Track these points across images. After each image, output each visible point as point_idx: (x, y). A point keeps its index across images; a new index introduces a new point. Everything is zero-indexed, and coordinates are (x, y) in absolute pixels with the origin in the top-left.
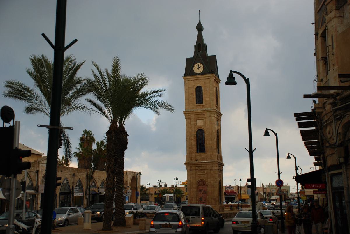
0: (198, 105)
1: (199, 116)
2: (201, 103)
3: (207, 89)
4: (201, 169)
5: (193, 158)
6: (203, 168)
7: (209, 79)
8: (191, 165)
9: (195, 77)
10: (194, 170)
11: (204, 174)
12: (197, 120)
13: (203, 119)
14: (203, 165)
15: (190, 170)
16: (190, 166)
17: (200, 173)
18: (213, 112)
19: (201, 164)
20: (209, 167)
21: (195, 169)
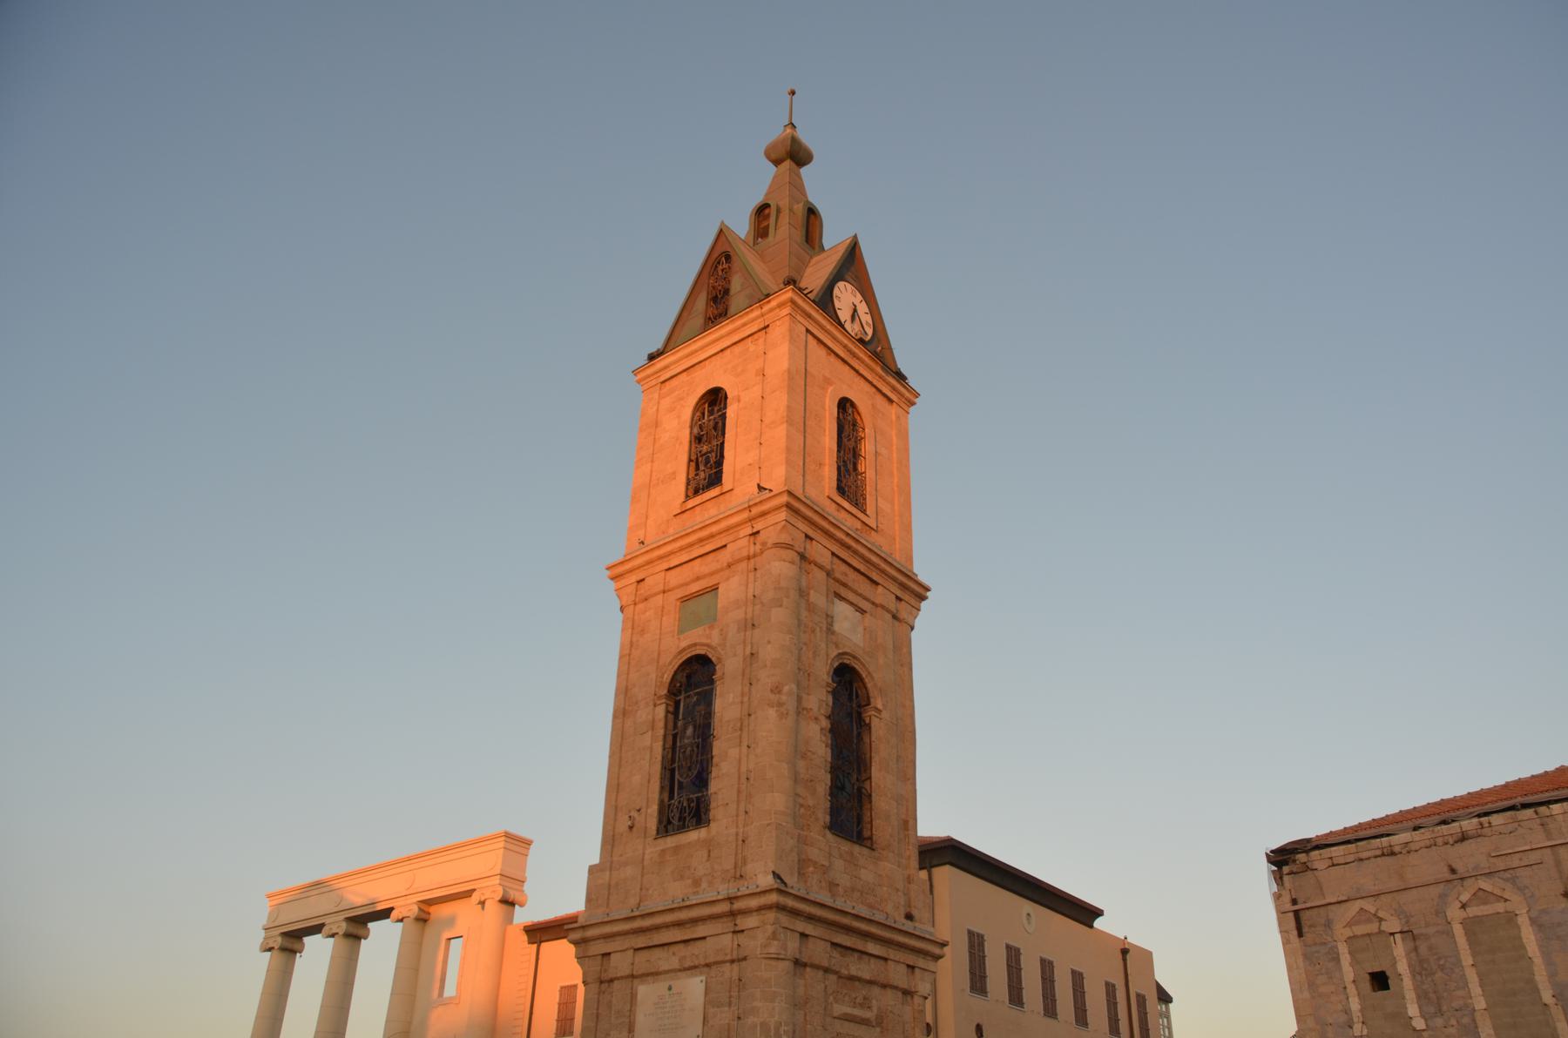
0: (846, 505)
1: (852, 575)
2: (856, 505)
3: (883, 451)
4: (854, 972)
5: (815, 863)
6: (864, 969)
7: (891, 401)
8: (810, 918)
9: (846, 341)
10: (816, 967)
11: (865, 1022)
12: (837, 601)
13: (863, 612)
14: (872, 948)
15: (798, 963)
16: (801, 926)
17: (849, 1010)
18: (913, 601)
19: (867, 936)
20: (898, 975)
21: (825, 964)
